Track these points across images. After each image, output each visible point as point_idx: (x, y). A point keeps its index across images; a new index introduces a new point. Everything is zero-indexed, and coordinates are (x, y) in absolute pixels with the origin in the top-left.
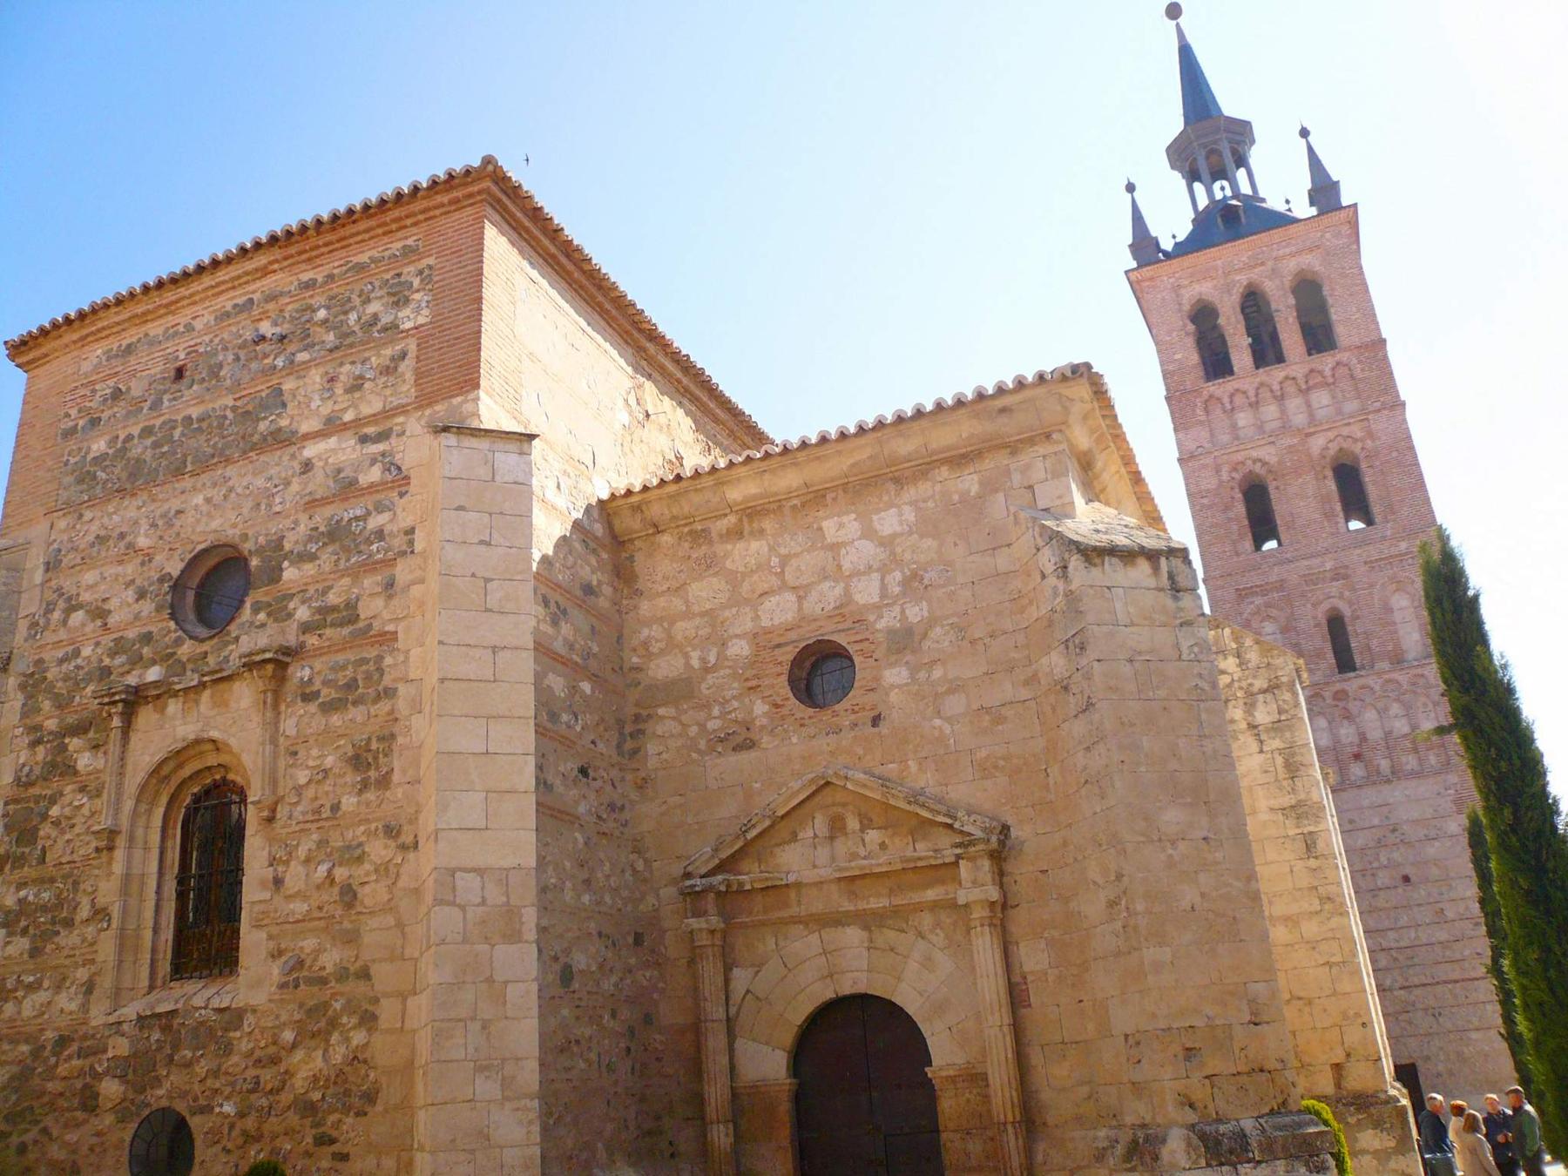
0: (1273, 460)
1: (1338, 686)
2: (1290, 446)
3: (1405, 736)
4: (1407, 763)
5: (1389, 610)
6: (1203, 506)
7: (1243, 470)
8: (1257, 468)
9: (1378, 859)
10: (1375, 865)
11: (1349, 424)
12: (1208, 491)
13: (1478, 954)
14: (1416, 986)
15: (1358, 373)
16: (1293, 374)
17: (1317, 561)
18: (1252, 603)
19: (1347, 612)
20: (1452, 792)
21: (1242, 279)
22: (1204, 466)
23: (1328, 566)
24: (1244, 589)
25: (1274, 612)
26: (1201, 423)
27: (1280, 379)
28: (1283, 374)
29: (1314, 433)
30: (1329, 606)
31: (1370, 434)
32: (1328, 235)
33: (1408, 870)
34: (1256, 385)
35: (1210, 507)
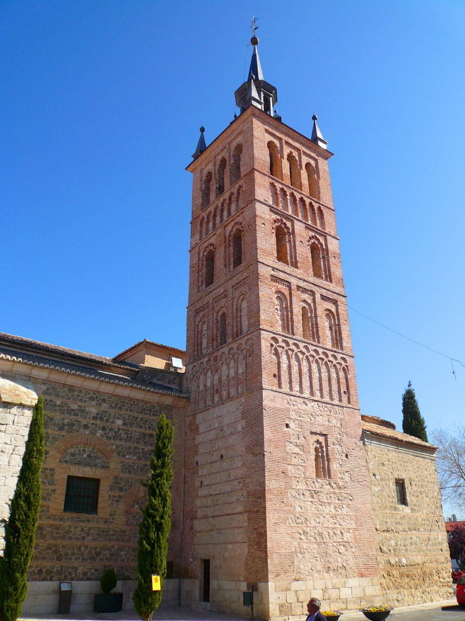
0: (214, 242)
5: (239, 310)
6: (193, 271)
7: (208, 250)
8: (212, 248)
9: (214, 446)
11: (238, 216)
13: (238, 500)
14: (216, 516)
17: (218, 290)
19: (226, 313)
20: (241, 407)
21: (219, 158)
23: (222, 291)
24: (198, 309)
25: (206, 319)
27: (221, 202)
28: (222, 199)
32: (245, 124)
33: (223, 452)
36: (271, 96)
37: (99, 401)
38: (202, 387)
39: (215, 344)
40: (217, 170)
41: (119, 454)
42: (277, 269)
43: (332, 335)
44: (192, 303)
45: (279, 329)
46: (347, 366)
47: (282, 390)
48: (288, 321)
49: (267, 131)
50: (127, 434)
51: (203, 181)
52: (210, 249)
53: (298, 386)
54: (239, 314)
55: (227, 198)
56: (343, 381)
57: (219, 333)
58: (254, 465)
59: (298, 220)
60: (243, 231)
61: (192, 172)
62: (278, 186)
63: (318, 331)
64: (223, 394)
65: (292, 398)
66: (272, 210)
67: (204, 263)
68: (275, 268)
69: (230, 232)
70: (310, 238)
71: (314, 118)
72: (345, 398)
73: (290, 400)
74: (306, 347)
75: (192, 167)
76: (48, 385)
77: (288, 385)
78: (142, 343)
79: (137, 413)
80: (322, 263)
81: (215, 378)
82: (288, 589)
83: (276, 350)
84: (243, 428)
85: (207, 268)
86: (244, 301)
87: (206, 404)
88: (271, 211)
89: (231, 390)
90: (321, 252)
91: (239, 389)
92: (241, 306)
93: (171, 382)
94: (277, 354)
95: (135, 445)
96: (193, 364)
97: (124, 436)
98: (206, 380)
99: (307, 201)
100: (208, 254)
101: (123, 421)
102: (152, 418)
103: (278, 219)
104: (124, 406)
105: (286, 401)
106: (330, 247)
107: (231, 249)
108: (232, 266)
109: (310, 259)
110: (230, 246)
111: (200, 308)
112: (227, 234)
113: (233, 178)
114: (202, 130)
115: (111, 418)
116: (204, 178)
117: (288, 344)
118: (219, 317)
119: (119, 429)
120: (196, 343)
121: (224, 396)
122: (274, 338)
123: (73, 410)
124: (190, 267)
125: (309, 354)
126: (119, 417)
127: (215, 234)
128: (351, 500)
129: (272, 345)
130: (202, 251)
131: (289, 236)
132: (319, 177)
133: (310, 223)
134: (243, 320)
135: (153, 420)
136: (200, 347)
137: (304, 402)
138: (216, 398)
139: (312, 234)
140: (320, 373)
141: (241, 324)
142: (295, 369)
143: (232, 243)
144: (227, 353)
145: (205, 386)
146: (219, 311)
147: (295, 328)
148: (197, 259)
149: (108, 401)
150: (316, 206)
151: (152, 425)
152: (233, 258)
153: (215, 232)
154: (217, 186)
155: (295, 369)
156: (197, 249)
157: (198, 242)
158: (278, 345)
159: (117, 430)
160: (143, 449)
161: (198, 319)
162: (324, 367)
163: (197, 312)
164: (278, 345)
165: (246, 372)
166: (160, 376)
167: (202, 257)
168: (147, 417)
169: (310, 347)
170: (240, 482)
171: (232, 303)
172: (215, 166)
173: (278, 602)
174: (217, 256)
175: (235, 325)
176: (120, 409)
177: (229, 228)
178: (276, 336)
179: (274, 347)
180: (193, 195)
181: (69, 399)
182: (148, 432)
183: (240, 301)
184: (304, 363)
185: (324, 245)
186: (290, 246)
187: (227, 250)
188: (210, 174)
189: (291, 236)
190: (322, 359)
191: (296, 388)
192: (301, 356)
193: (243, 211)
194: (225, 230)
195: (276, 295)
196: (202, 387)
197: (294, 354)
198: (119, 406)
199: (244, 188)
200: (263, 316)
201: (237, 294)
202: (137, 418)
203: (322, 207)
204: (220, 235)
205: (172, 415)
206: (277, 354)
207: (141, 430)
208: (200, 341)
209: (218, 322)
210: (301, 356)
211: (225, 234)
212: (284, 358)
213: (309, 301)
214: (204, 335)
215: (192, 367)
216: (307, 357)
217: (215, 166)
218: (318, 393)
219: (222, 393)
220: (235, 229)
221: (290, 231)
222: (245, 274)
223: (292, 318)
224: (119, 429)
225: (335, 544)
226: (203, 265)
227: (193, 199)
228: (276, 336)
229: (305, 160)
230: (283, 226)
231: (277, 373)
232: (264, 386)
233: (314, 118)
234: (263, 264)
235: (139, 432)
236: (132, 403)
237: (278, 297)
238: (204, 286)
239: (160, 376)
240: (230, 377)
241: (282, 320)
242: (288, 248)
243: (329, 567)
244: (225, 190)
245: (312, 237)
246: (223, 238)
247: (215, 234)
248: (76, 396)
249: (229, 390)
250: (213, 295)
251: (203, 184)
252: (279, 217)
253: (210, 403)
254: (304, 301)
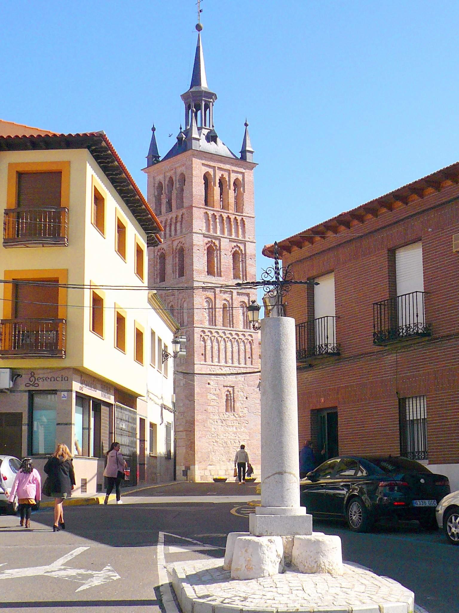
29: (175, 240)
36: (211, 101)
42: (206, 282)
43: (244, 319)
45: (206, 324)
46: (252, 340)
47: (206, 363)
48: (212, 316)
49: (203, 164)
51: (156, 187)
53: (217, 359)
56: (249, 350)
58: (189, 406)
62: (210, 213)
63: (233, 320)
65: (213, 367)
66: (205, 236)
67: (158, 261)
70: (233, 248)
71: (246, 125)
72: (249, 361)
73: (211, 368)
74: (224, 333)
77: (211, 359)
80: (241, 265)
82: (205, 469)
83: (203, 338)
84: (184, 385)
86: (185, 302)
88: (204, 236)
90: (240, 257)
94: (204, 340)
99: (232, 217)
103: (209, 241)
105: (209, 369)
106: (247, 251)
107: (177, 259)
109: (232, 265)
112: (174, 247)
113: (178, 200)
114: (154, 129)
116: (156, 185)
117: (211, 333)
122: (202, 331)
125: (226, 336)
128: (247, 424)
129: (201, 336)
130: (156, 251)
131: (217, 252)
132: (244, 189)
137: (220, 368)
140: (232, 348)
142: (216, 348)
143: (177, 255)
147: (217, 321)
150: (239, 218)
154: (166, 201)
155: (216, 348)
158: (205, 335)
162: (236, 343)
164: (205, 335)
169: (227, 332)
170: (182, 415)
171: (178, 302)
173: (200, 475)
178: (204, 329)
179: (202, 337)
184: (222, 343)
185: (243, 250)
186: (217, 259)
188: (160, 183)
189: (218, 252)
190: (235, 338)
191: (216, 360)
192: (219, 339)
195: (205, 300)
197: (215, 338)
199: (185, 216)
200: (196, 318)
206: (204, 340)
210: (219, 339)
211: (173, 246)
212: (209, 343)
213: (228, 299)
216: (224, 339)
218: (230, 361)
221: (218, 248)
223: (215, 314)
225: (234, 448)
226: (157, 262)
228: (204, 329)
229: (233, 176)
230: (212, 245)
231: (204, 353)
232: (195, 363)
233: (246, 125)
234: (197, 281)
237: (207, 301)
241: (209, 316)
242: (216, 262)
243: (230, 459)
252: (210, 240)
254: (225, 300)
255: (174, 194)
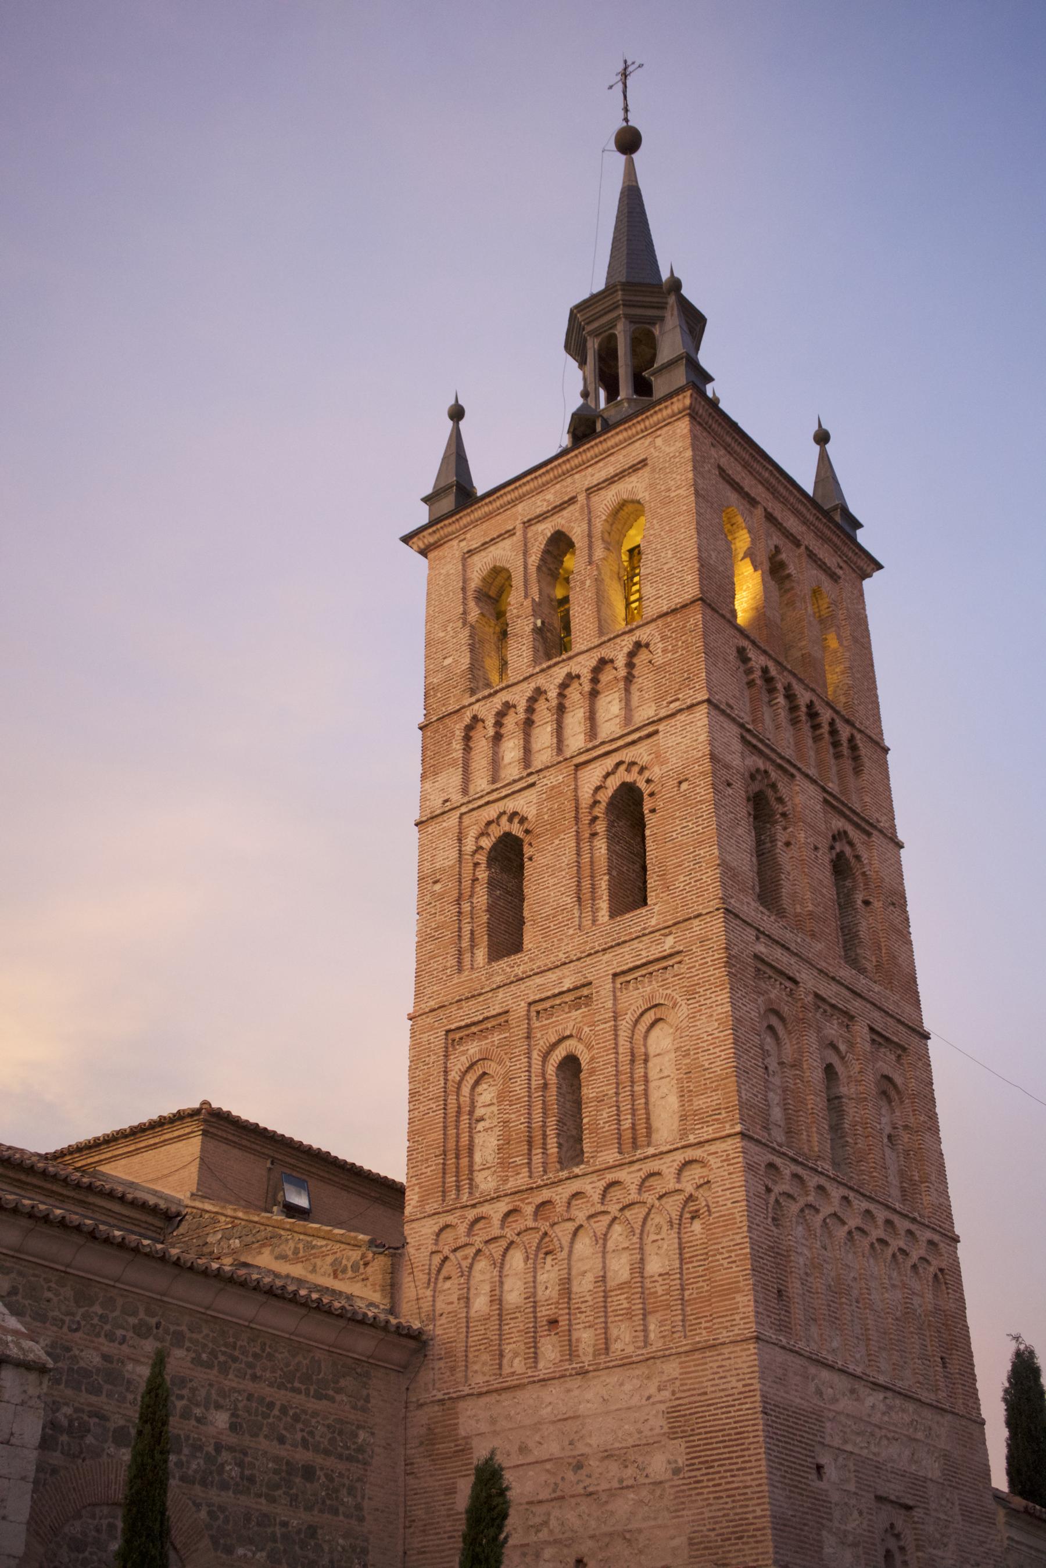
0: (531, 812)
1: (546, 1194)
2: (553, 788)
3: (621, 1287)
4: (618, 1338)
6: (433, 893)
7: (496, 832)
8: (516, 829)
10: (544, 1535)
12: (443, 870)
15: (659, 659)
16: (575, 670)
17: (552, 976)
18: (464, 1053)
20: (666, 1394)
22: (445, 831)
23: (567, 984)
24: (459, 1028)
25: (492, 1067)
26: (453, 763)
30: (564, 1054)
31: (659, 757)
34: (529, 694)
35: (440, 896)
37: (162, 1340)
38: (480, 1304)
39: (537, 1159)
40: (532, 569)
41: (215, 1542)
44: (432, 1004)
50: (240, 1464)
51: (470, 593)
52: (507, 829)
54: (639, 1071)
55: (586, 674)
57: (552, 1122)
59: (807, 776)
60: (652, 794)
61: (424, 552)
64: (578, 1340)
67: (483, 875)
68: (763, 933)
69: (598, 789)
75: (428, 538)
76: (13, 1275)
78: (194, 1113)
79: (271, 1385)
81: (542, 1278)
84: (676, 1471)
85: (490, 893)
87: (500, 1368)
89: (614, 1332)
91: (652, 1327)
92: (645, 1045)
93: (344, 1271)
95: (264, 1505)
96: (442, 1220)
97: (232, 1471)
98: (501, 1283)
100: (494, 848)
101: (233, 1415)
102: (313, 1405)
104: (235, 1359)
107: (601, 846)
108: (604, 905)
110: (594, 835)
111: (468, 1026)
114: (457, 413)
115: (198, 1405)
118: (551, 1069)
119: (218, 1448)
120: (451, 1144)
121: (582, 1345)
123: (86, 1373)
124: (421, 879)
126: (221, 1400)
127: (533, 785)
130: (472, 833)
133: (832, 786)
134: (654, 1096)
135: (315, 1414)
136: (464, 1161)
138: (550, 1350)
139: (839, 824)
141: (647, 1103)
143: (601, 827)
144: (596, 1197)
145: (497, 1300)
146: (554, 1046)
148: (454, 854)
149: (191, 1340)
151: (311, 1433)
152: (606, 877)
153: (531, 780)
154: (535, 624)
156: (452, 820)
157: (457, 798)
159: (211, 1449)
160: (285, 1524)
161: (459, 1063)
163: (455, 1037)
165: (681, 1273)
166: (291, 1244)
167: (475, 852)
168: (299, 1399)
171: (616, 1029)
172: (525, 553)
174: (540, 860)
175: (625, 1106)
176: (224, 1369)
177: (591, 776)
180: (428, 633)
181: (76, 1330)
182: (303, 1456)
183: (642, 1027)
187: (585, 846)
193: (656, 732)
194: (576, 779)
196: (480, 1304)
198: (222, 1358)
201: (634, 999)
202: (271, 1405)
203: (858, 736)
204: (554, 792)
205: (367, 1400)
207: (283, 1452)
208: (464, 1140)
209: (545, 1086)
214: (482, 1119)
215: (436, 1229)
217: (525, 553)
219: (575, 1335)
220: (613, 783)
222: (670, 941)
224: (218, 1448)
226: (475, 880)
227: (428, 645)
235: (277, 1459)
236: (258, 1350)
238: (481, 954)
239: (291, 1244)
240: (611, 1284)
244: (577, 647)
245: (839, 836)
246: (569, 805)
247: (533, 785)
248: (96, 1321)
249: (606, 1328)
250: (532, 989)
251: (472, 604)
253: (518, 1365)
255: (583, 583)
